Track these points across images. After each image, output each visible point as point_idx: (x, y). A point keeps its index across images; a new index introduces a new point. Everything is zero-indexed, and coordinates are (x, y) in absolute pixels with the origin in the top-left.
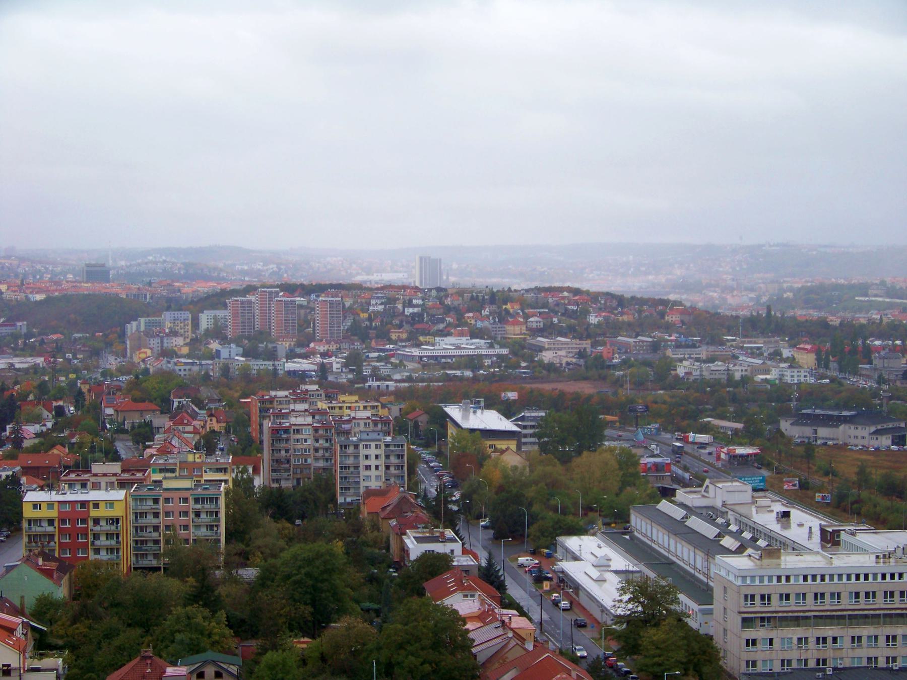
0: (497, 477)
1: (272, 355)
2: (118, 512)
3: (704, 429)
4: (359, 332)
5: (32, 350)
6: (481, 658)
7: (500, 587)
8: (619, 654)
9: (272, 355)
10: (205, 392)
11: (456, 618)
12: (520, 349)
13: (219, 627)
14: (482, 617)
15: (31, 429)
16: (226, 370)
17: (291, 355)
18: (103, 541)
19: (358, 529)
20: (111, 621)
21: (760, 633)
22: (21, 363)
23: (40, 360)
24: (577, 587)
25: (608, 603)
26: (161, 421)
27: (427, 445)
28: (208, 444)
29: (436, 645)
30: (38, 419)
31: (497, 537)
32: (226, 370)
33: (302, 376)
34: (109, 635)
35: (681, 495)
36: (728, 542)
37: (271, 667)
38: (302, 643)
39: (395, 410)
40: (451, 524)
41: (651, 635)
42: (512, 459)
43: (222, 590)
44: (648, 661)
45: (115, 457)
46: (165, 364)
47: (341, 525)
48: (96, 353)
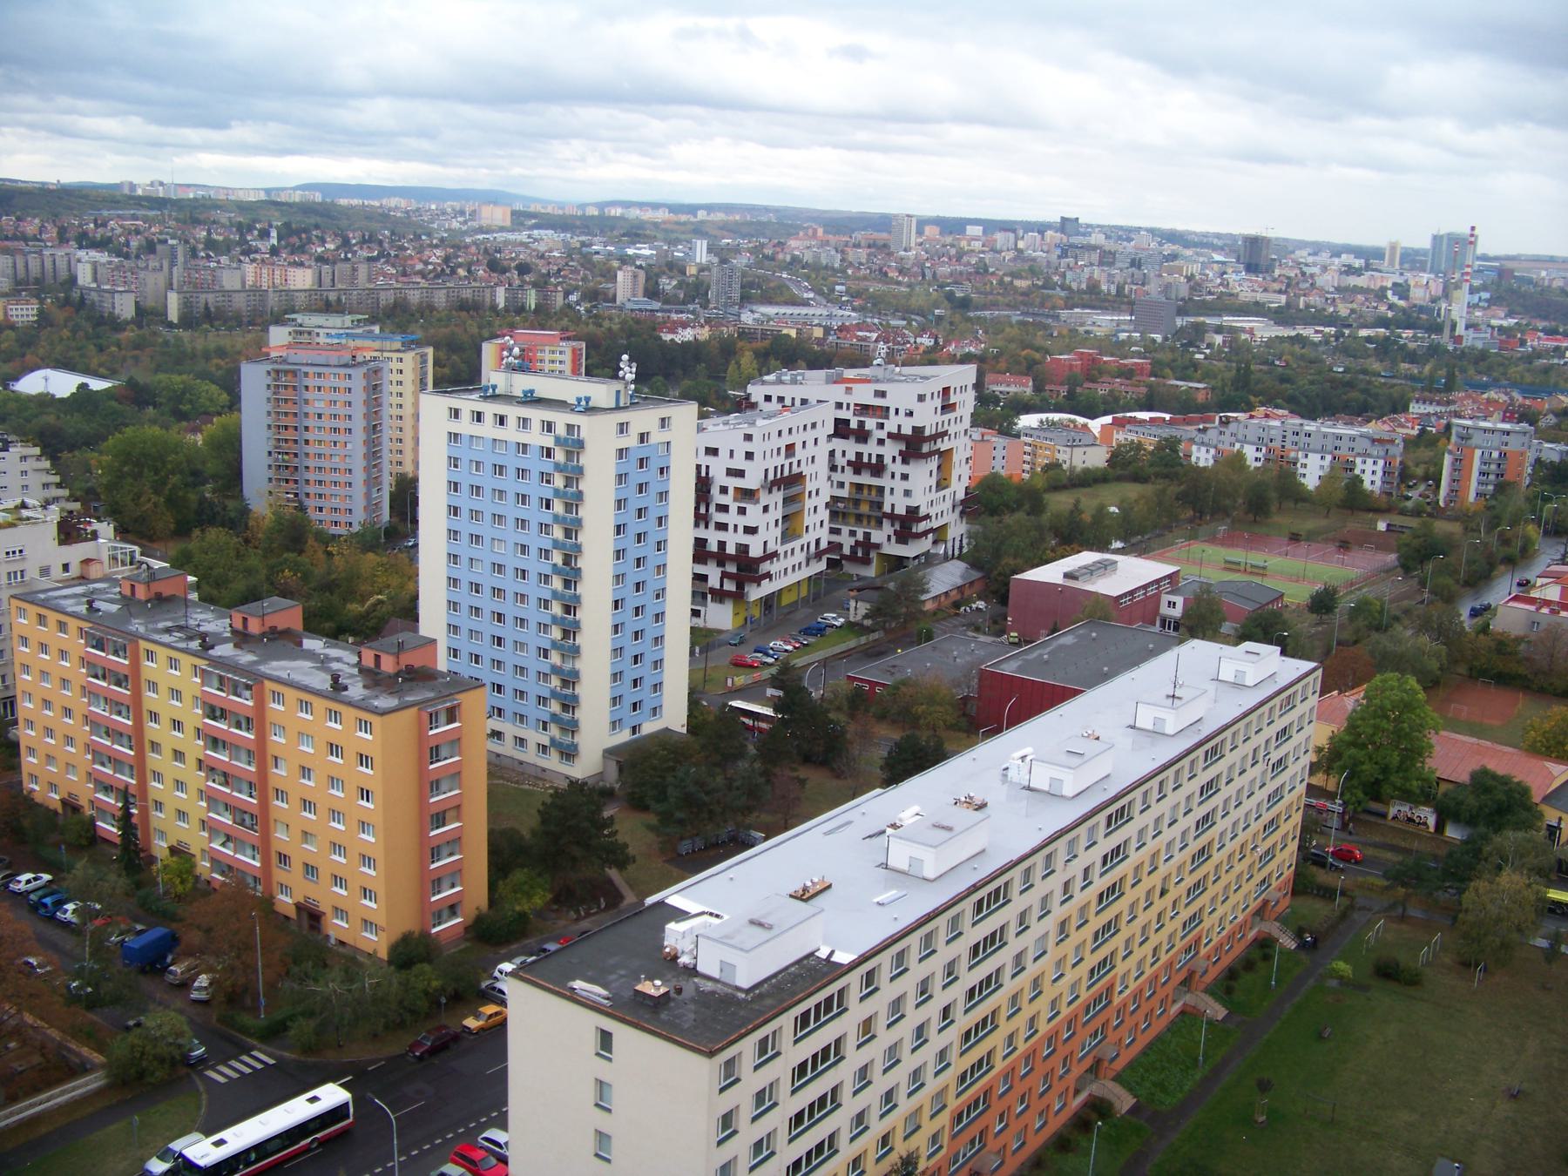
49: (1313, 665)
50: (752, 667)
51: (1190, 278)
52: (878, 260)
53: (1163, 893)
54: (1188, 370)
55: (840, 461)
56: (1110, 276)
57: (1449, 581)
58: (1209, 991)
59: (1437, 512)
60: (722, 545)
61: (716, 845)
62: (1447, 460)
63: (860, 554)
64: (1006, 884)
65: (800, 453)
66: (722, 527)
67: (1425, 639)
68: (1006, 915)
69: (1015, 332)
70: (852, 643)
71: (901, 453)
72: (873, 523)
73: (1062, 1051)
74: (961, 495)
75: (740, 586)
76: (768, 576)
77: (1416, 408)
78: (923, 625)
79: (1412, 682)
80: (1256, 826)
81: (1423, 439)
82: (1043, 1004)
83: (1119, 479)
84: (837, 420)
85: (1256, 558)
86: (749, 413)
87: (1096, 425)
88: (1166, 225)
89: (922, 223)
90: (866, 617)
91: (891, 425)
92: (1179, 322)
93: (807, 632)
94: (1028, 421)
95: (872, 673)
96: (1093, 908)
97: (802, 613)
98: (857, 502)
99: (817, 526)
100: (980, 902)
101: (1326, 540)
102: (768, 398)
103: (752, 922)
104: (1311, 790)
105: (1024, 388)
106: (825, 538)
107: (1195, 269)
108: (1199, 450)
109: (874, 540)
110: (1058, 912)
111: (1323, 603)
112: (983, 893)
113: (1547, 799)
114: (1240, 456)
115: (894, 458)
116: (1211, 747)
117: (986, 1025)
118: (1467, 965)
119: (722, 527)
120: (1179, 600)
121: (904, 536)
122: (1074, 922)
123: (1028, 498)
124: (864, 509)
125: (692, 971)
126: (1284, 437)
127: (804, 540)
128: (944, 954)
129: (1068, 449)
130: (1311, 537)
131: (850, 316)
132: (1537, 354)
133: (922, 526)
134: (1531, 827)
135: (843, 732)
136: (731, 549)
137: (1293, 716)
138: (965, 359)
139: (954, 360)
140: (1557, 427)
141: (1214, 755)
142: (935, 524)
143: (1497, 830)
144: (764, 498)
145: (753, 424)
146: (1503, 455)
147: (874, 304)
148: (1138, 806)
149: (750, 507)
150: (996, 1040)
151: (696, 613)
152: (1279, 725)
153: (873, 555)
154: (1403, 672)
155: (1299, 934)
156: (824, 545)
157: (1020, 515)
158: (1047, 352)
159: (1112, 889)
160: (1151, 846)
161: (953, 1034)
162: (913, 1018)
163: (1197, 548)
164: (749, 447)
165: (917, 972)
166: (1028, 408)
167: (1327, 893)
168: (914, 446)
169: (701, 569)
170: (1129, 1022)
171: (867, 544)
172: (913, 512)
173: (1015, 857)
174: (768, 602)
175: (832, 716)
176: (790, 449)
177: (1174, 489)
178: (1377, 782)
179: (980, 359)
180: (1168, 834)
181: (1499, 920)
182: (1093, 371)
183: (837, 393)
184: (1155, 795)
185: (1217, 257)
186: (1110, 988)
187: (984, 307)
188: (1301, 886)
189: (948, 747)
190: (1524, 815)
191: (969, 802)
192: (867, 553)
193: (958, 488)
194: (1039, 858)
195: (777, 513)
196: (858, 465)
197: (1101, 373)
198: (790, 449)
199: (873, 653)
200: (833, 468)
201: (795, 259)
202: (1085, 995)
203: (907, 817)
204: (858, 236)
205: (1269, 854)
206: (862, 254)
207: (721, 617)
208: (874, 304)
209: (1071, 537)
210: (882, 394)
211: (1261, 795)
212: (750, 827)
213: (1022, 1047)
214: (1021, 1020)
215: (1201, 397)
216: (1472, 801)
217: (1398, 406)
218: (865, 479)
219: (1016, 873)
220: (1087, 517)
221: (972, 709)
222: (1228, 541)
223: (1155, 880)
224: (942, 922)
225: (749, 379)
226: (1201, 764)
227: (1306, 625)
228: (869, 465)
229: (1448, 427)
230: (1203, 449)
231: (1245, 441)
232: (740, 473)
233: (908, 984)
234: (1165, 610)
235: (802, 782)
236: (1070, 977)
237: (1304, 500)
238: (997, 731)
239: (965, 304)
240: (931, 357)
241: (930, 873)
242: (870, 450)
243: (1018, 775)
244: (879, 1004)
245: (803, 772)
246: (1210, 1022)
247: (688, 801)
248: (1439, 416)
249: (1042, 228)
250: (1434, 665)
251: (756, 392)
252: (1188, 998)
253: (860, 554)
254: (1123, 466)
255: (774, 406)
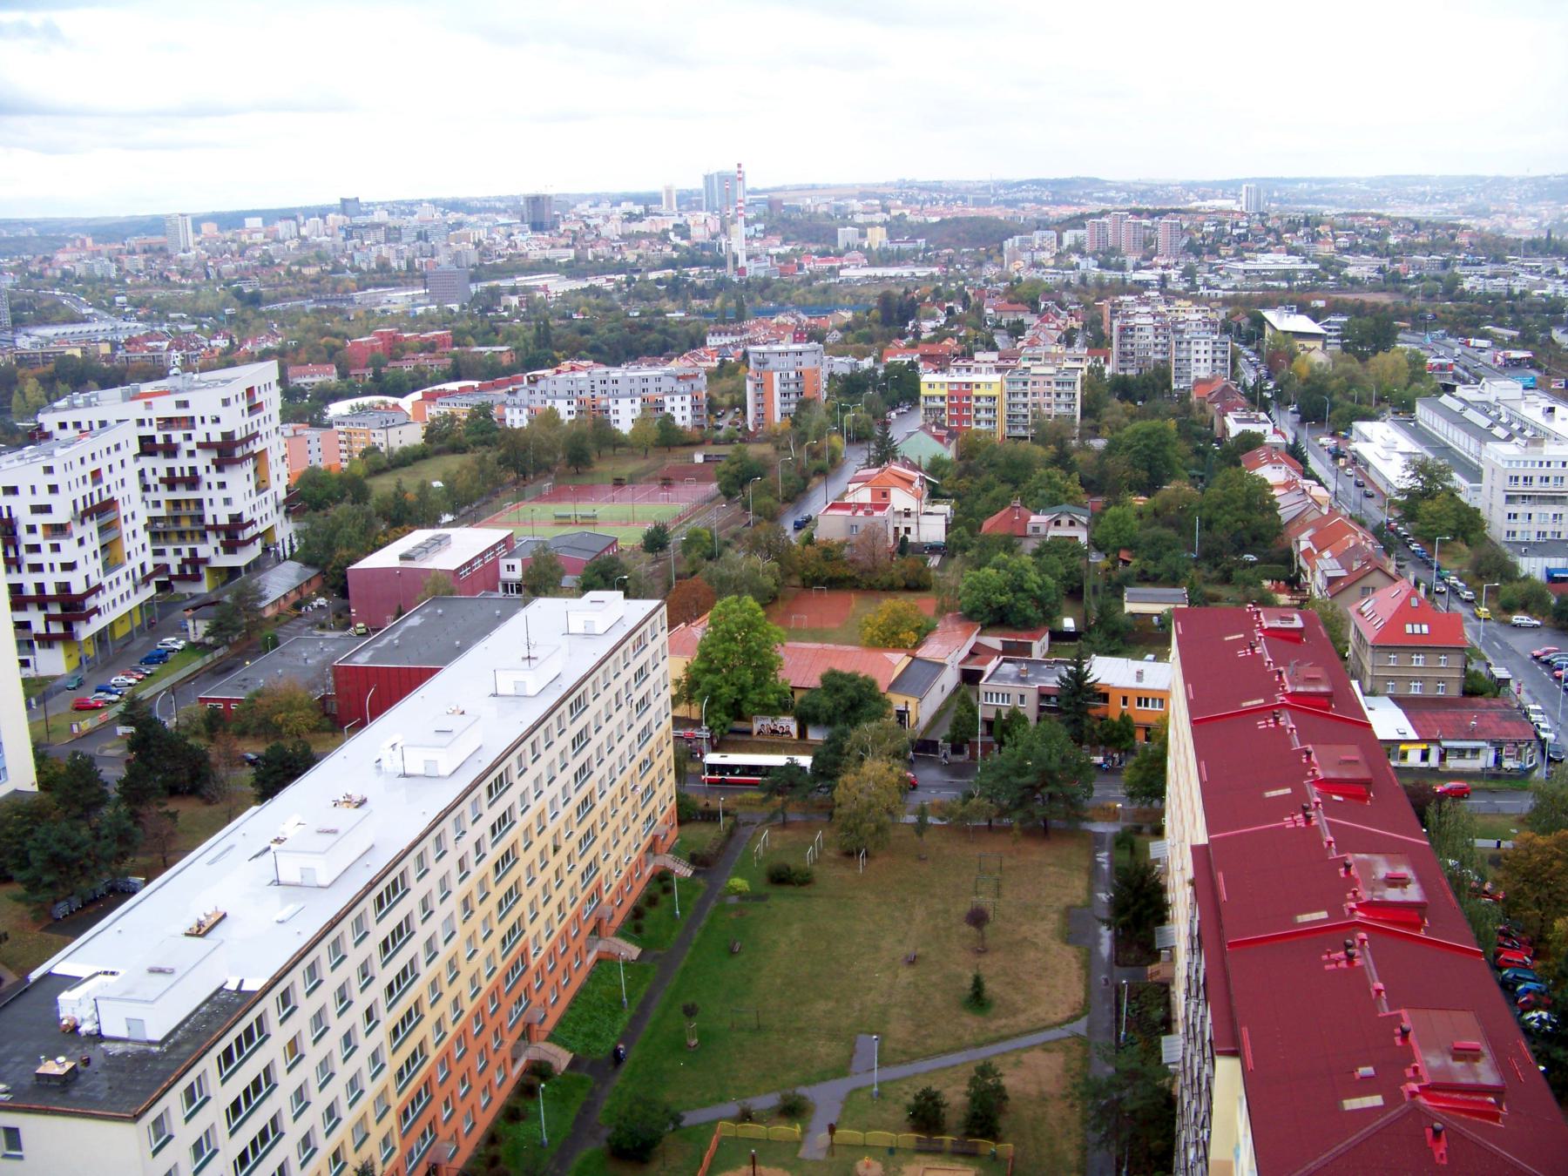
0: (1305, 372)
1: (1121, 267)
2: (995, 391)
3: (1484, 336)
4: (1194, 249)
5: (927, 262)
6: (1285, 519)
7: (1304, 461)
8: (1399, 521)
9: (1121, 267)
10: (1066, 297)
11: (1264, 485)
12: (1328, 265)
13: (1073, 485)
14: (1287, 485)
15: (927, 325)
16: (1083, 279)
17: (1137, 267)
18: (983, 415)
19: (1188, 410)
20: (990, 477)
21: (1521, 509)
22: (921, 272)
23: (936, 270)
24: (1367, 465)
25: (1392, 479)
26: (1030, 319)
27: (1247, 344)
28: (1068, 339)
29: (1249, 507)
30: (933, 317)
31: (1303, 421)
32: (1083, 279)
33: (1146, 285)
34: (987, 489)
35: (1460, 390)
36: (1499, 431)
37: (1114, 519)
38: (1140, 501)
39: (1222, 314)
40: (1265, 407)
41: (1428, 506)
42: (1317, 356)
43: (1076, 457)
44: (1424, 528)
45: (993, 347)
46: (1034, 274)
47: (1174, 407)
48: (980, 264)
49: (656, 602)
50: (95, 708)
51: (478, 244)
52: (158, 264)
53: (556, 850)
54: (490, 334)
55: (152, 480)
56: (399, 252)
57: (769, 500)
58: (621, 933)
59: (748, 437)
60: (40, 587)
61: (94, 901)
62: (750, 386)
63: (189, 572)
64: (402, 874)
65: (107, 478)
66: (37, 568)
67: (757, 560)
68: (408, 905)
69: (310, 321)
70: (197, 664)
71: (214, 461)
72: (197, 538)
73: (492, 1025)
74: (283, 495)
75: (68, 627)
76: (97, 610)
77: (713, 341)
78: (268, 632)
79: (750, 601)
80: (632, 767)
81: (724, 370)
82: (463, 983)
83: (439, 453)
84: (141, 438)
85: (584, 508)
86: (45, 444)
87: (407, 403)
88: (448, 194)
89: (198, 222)
90: (207, 634)
91: (199, 435)
92: (474, 288)
93: (149, 661)
94: (338, 409)
95: (225, 691)
96: (492, 879)
97: (137, 645)
98: (177, 519)
99: (138, 551)
100: (380, 897)
101: (649, 480)
102: (63, 426)
103: (152, 971)
104: (677, 722)
105: (327, 376)
106: (150, 562)
107: (482, 234)
108: (512, 412)
109: (200, 555)
110: (459, 891)
111: (656, 541)
112: (381, 888)
113: (893, 687)
114: (553, 413)
115: (208, 468)
116: (574, 699)
117: (411, 1017)
118: (850, 854)
119: (37, 568)
120: (517, 563)
121: (231, 545)
122: (476, 897)
123: (352, 487)
124: (186, 525)
125: (98, 1037)
126: (593, 387)
127: (128, 567)
128: (355, 957)
129: (383, 432)
130: (633, 479)
131: (139, 328)
132: (815, 276)
133: (248, 533)
134: (883, 715)
135: (205, 757)
136: (51, 590)
137: (646, 655)
138: (265, 356)
139: (252, 358)
140: (844, 341)
141: (579, 706)
142: (261, 528)
143: (855, 723)
144: (78, 531)
145: (52, 454)
146: (799, 374)
147: (159, 312)
148: (515, 771)
149: (63, 543)
150: (425, 1029)
151: (25, 663)
152: (635, 666)
153: (203, 570)
154: (740, 594)
155: (694, 860)
156: (149, 569)
157: (345, 506)
158: (347, 337)
159: (506, 856)
160: (535, 806)
161: (382, 1034)
162: (338, 1027)
163: (526, 508)
164: (52, 480)
165: (332, 981)
166: (336, 396)
167: (710, 816)
168: (226, 452)
169: (22, 616)
170: (550, 982)
171: (195, 561)
172: (236, 520)
173: (405, 846)
174: (101, 638)
175: (190, 742)
176: (96, 475)
177: (492, 455)
178: (737, 703)
179: (280, 354)
180: (550, 792)
181: (871, 806)
182: (395, 349)
183: (137, 409)
184: (529, 757)
185: (502, 220)
186: (524, 953)
187: (275, 300)
188: (686, 813)
189: (315, 750)
190: (875, 706)
191: (348, 801)
192: (196, 570)
193: (279, 488)
194: (429, 842)
195: (94, 544)
196: (171, 482)
197: (404, 350)
198: (96, 475)
199: (222, 670)
200: (146, 488)
201: (66, 274)
202: (501, 966)
203: (289, 830)
204: (132, 242)
205: (649, 792)
206: (139, 260)
207: (53, 662)
208: (159, 312)
209: (402, 517)
210: (185, 404)
211: (631, 736)
212: (127, 874)
213: (451, 1030)
214: (445, 1005)
215: (506, 360)
216: (827, 702)
217: (697, 342)
218: (182, 494)
219: (410, 861)
220: (411, 496)
221: (333, 708)
222: (556, 496)
223: (547, 839)
224: (346, 925)
225: (38, 409)
226: (568, 718)
227: (643, 565)
228: (183, 480)
229: (746, 355)
230: (516, 411)
231: (555, 396)
232: (47, 509)
233: (326, 995)
234: (505, 575)
235: (174, 816)
236: (484, 951)
237: (622, 445)
238: (362, 724)
239: (255, 300)
240: (229, 359)
241: (324, 880)
242: (181, 463)
243: (392, 764)
244: (301, 1022)
245: (172, 806)
246: (627, 963)
247: (55, 861)
248: (735, 345)
249: (323, 213)
250: (769, 582)
251: (49, 421)
252: (602, 946)
253: (189, 572)
254: (440, 440)
255: (71, 432)
